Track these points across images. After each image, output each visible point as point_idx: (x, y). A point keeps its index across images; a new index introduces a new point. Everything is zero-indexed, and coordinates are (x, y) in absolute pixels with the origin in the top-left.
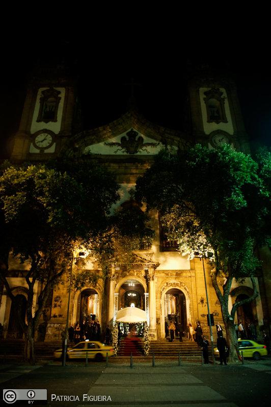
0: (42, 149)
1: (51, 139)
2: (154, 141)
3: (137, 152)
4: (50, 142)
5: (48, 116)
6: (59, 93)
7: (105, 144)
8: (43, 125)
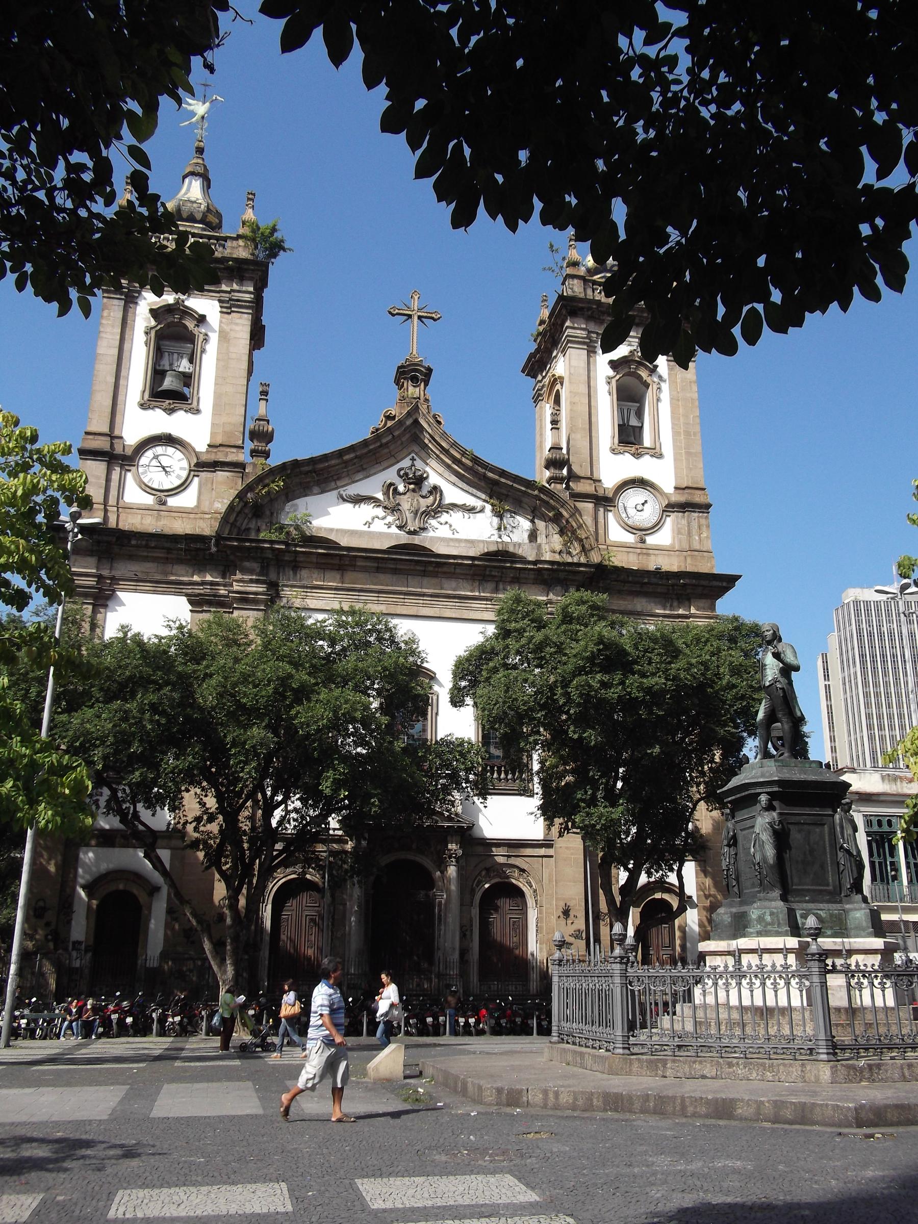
1: (185, 464)
2: (471, 501)
3: (424, 529)
4: (184, 474)
5: (170, 392)
8: (158, 421)
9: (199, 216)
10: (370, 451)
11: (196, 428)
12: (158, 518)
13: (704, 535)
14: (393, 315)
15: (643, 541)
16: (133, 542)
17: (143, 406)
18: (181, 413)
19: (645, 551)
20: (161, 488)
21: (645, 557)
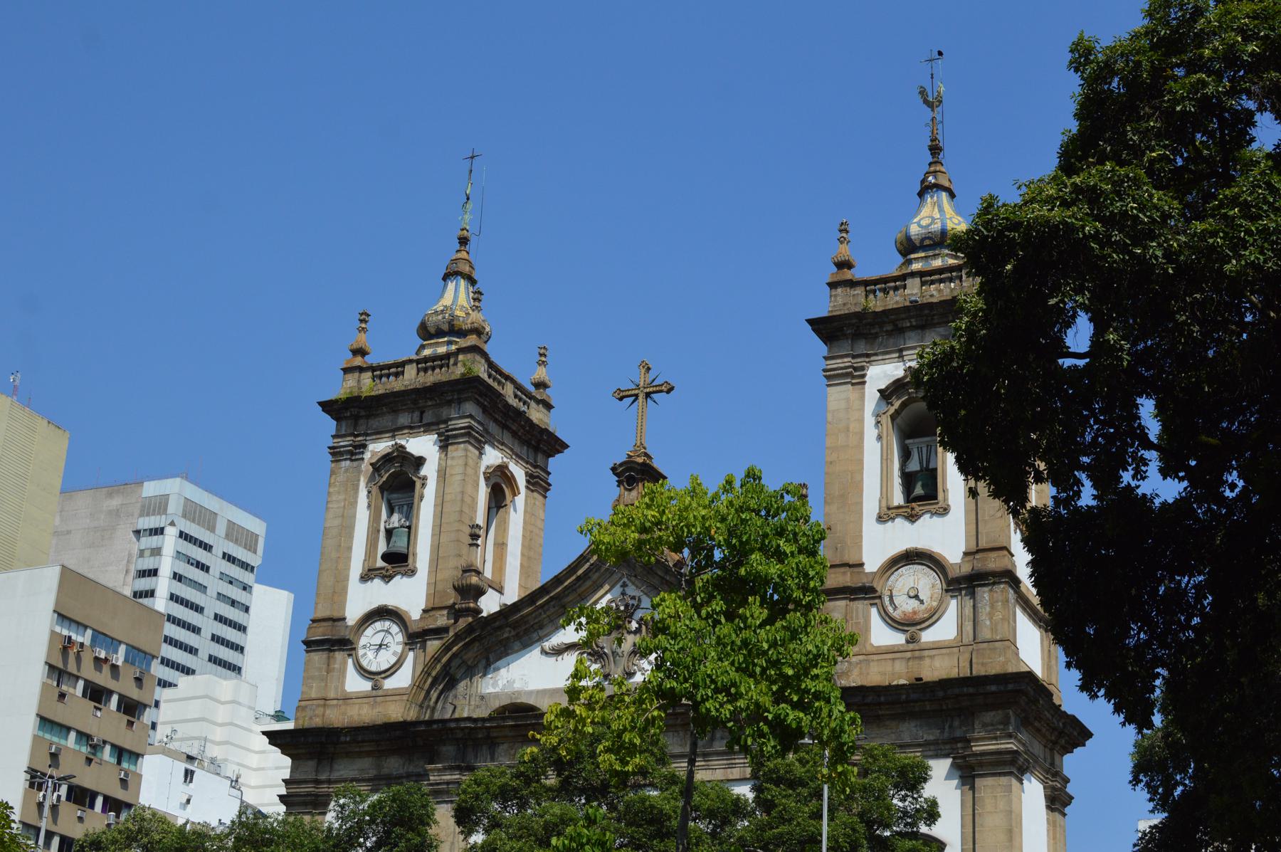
6: (420, 461)
7: (544, 652)
9: (445, 327)
11: (410, 595)
12: (373, 707)
13: (998, 616)
15: (912, 640)
16: (343, 739)
17: (366, 577)
18: (398, 577)
19: (917, 653)
21: (917, 662)
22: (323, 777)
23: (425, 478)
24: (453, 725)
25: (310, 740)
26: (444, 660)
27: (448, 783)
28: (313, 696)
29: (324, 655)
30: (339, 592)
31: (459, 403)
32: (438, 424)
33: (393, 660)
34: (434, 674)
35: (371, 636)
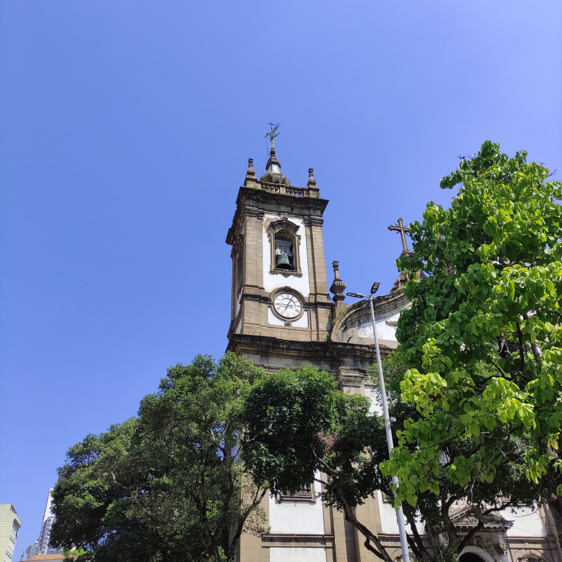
0: (288, 321)
6: (297, 228)
7: (387, 323)
10: (401, 297)
11: (302, 284)
12: (289, 334)
14: (391, 230)
16: (281, 346)
18: (292, 276)
20: (288, 317)
22: (265, 365)
23: (300, 236)
24: (358, 348)
25: (263, 343)
26: (347, 316)
27: (356, 377)
28: (253, 322)
29: (257, 303)
30: (259, 275)
31: (314, 210)
32: (304, 215)
33: (297, 314)
34: (342, 321)
35: (281, 300)
